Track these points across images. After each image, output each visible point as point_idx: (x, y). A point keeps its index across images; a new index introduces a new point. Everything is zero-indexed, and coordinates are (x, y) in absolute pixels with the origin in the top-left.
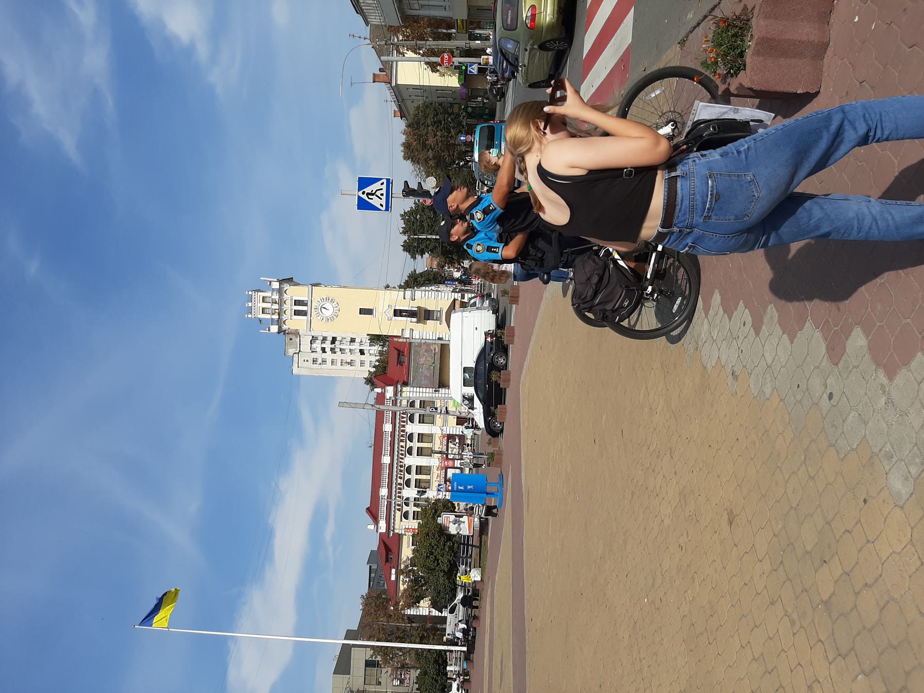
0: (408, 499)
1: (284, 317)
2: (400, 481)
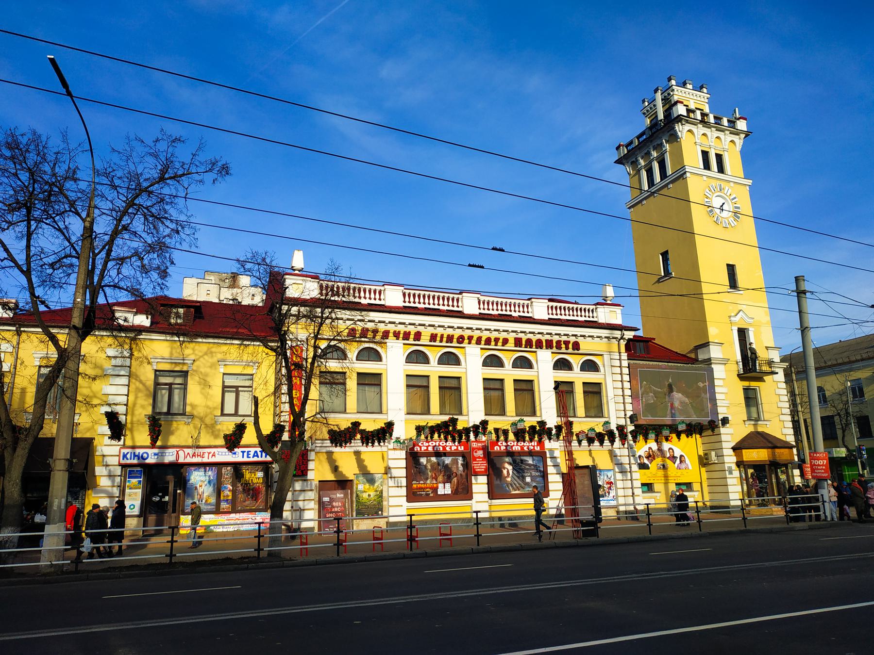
0: (378, 357)
1: (700, 130)
2: (425, 339)
